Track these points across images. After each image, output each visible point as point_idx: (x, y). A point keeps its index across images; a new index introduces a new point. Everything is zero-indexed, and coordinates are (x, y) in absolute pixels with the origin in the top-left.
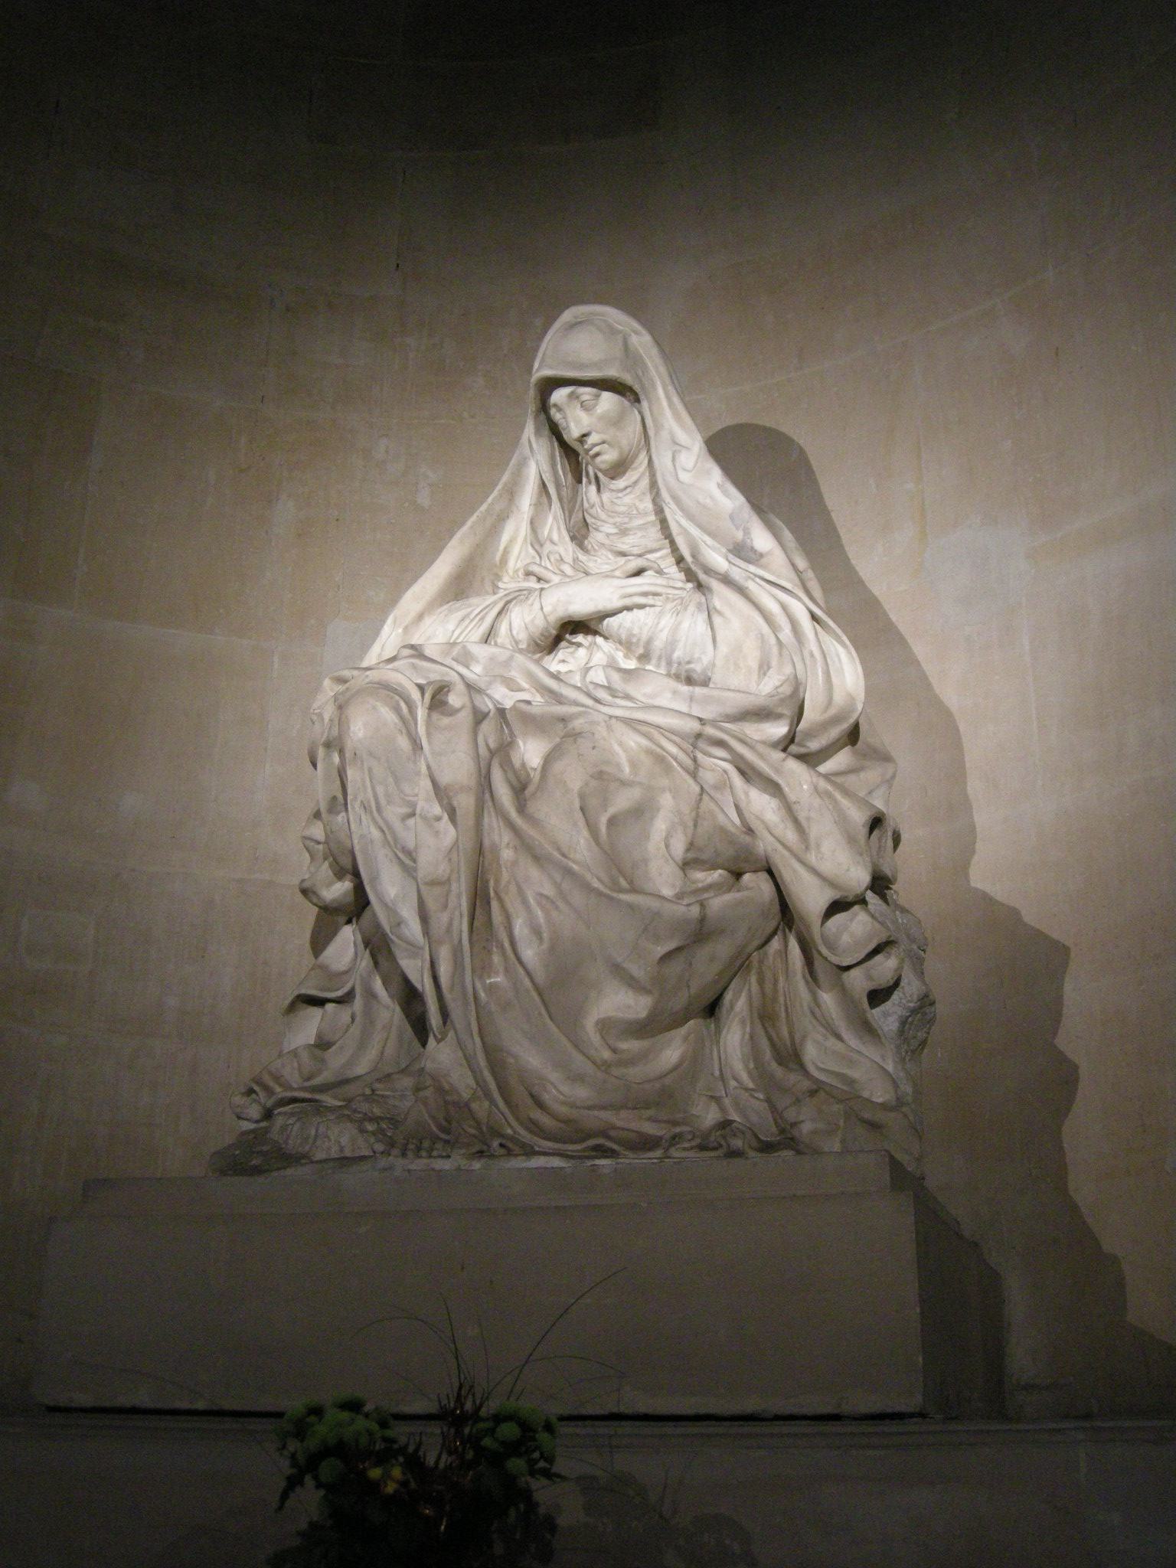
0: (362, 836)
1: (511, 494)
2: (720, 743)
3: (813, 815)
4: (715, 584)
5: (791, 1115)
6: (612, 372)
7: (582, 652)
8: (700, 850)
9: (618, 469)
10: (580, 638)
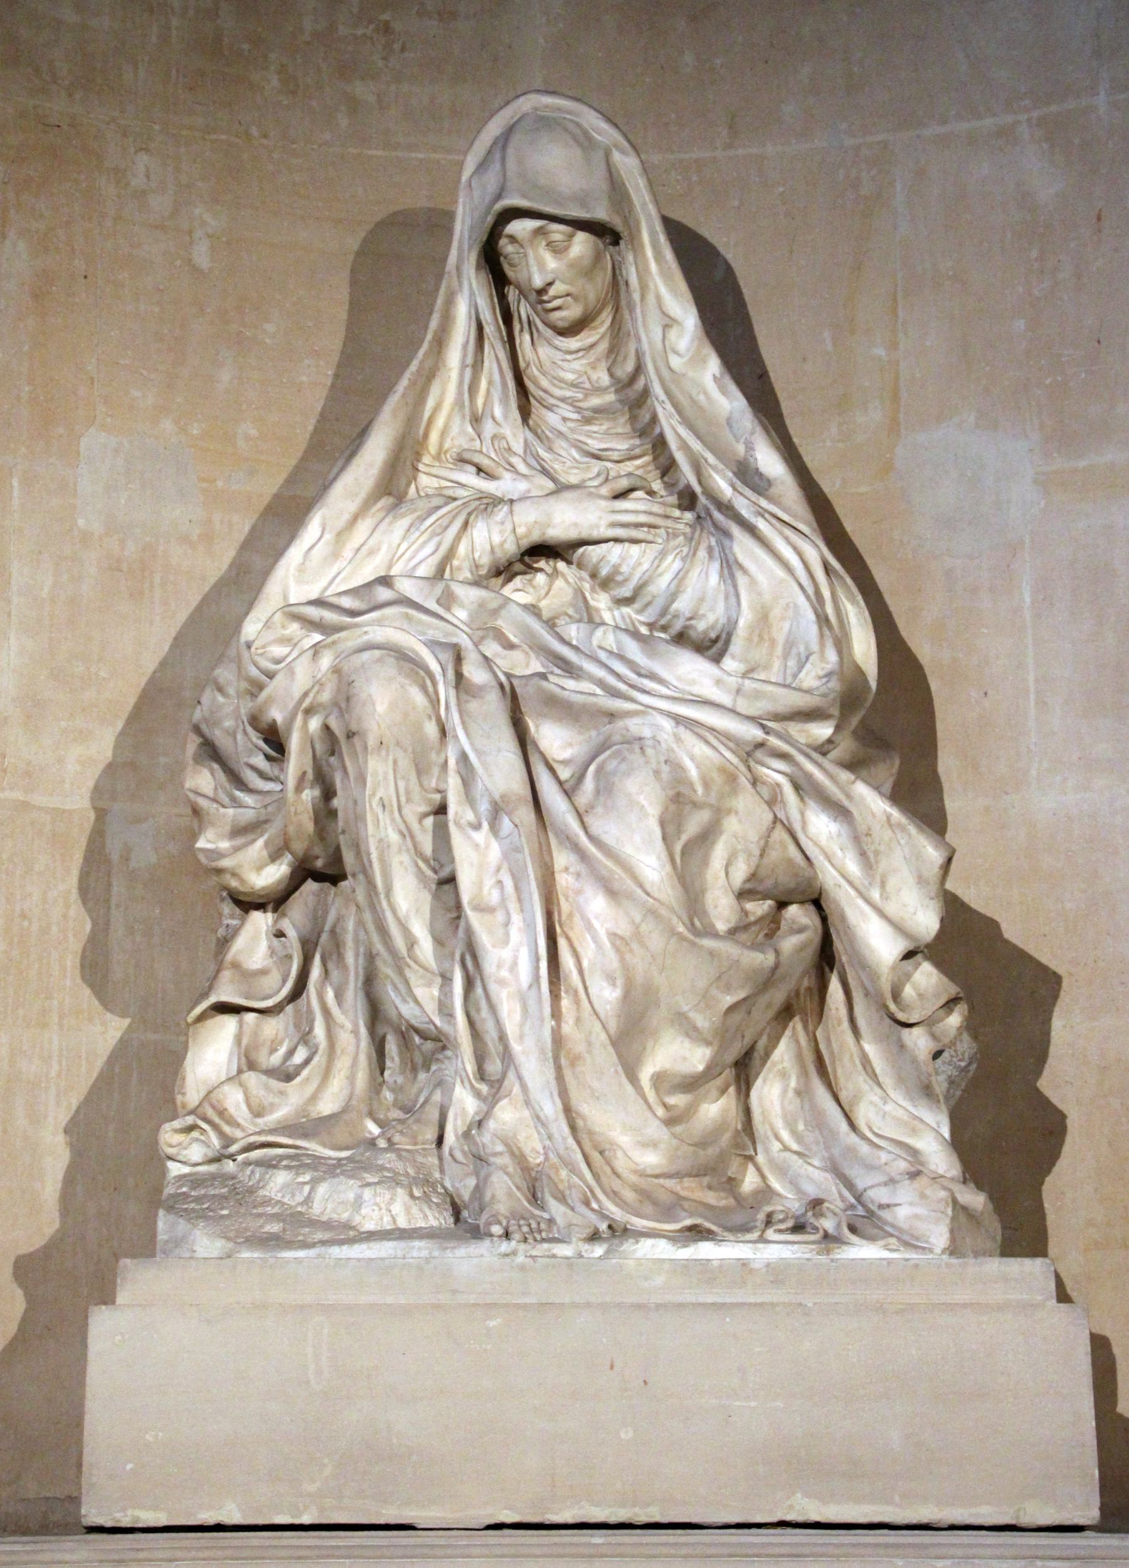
0: (381, 841)
1: (440, 343)
2: (783, 756)
3: (882, 848)
4: (736, 530)
5: (879, 1195)
6: (601, 213)
7: (540, 578)
8: (761, 881)
10: (542, 564)
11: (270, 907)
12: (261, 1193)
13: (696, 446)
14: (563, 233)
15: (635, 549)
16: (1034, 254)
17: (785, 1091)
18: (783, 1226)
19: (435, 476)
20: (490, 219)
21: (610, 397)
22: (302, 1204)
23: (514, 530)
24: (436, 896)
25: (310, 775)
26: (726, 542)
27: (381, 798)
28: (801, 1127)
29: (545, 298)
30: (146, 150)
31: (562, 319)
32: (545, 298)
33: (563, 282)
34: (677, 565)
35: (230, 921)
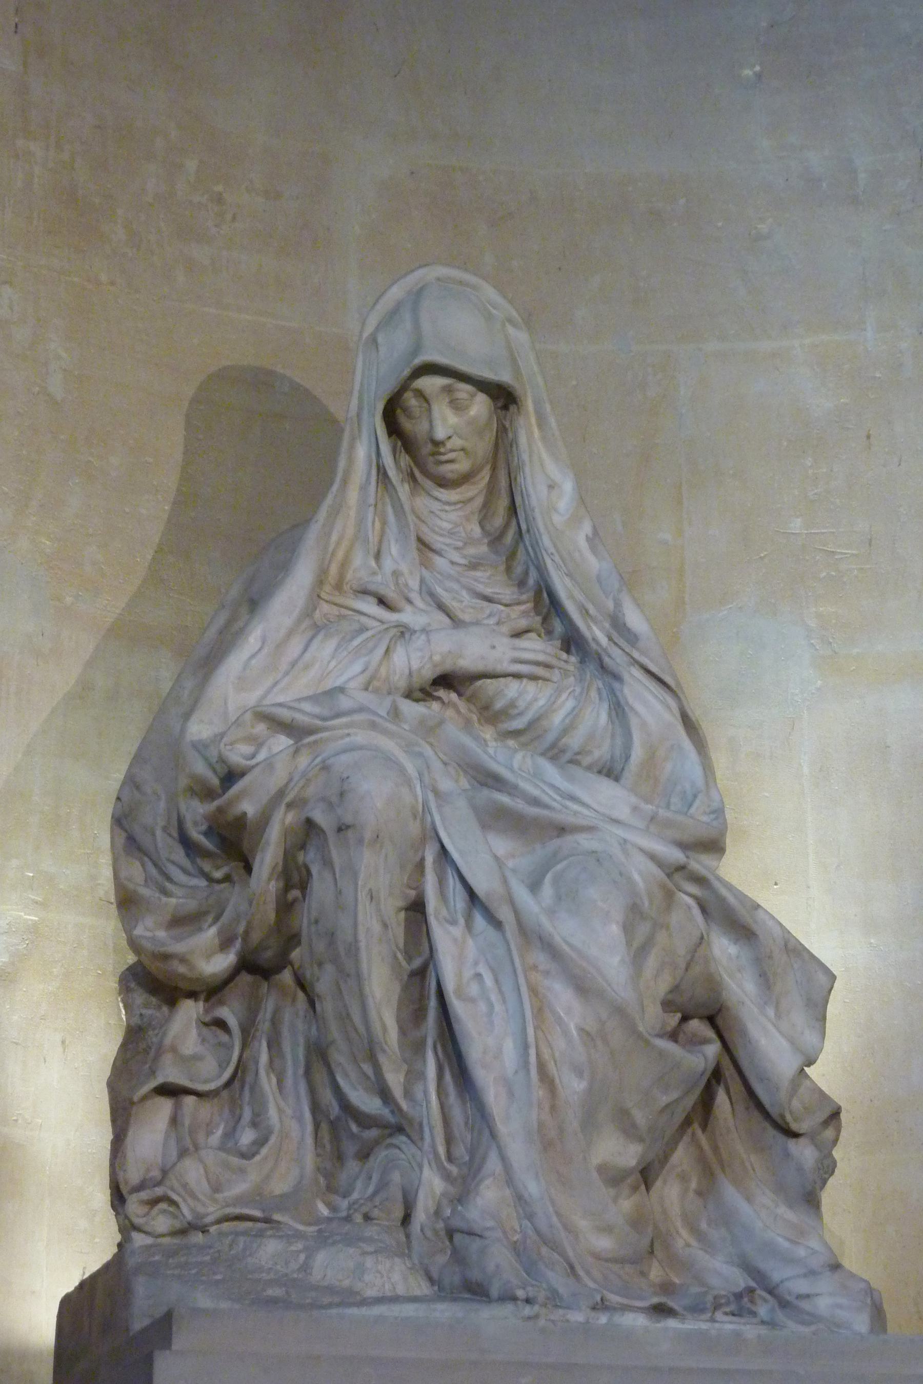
5: (801, 1286)
6: (504, 377)
11: (202, 997)
13: (580, 597)
14: (467, 392)
17: (685, 1191)
18: (728, 1310)
19: (335, 604)
20: (407, 372)
21: (484, 549)
22: (299, 1270)
23: (431, 657)
24: (405, 988)
25: (280, 868)
26: (616, 685)
27: (370, 890)
29: (442, 450)
30: (10, 283)
31: (452, 472)
33: (460, 437)
34: (570, 704)
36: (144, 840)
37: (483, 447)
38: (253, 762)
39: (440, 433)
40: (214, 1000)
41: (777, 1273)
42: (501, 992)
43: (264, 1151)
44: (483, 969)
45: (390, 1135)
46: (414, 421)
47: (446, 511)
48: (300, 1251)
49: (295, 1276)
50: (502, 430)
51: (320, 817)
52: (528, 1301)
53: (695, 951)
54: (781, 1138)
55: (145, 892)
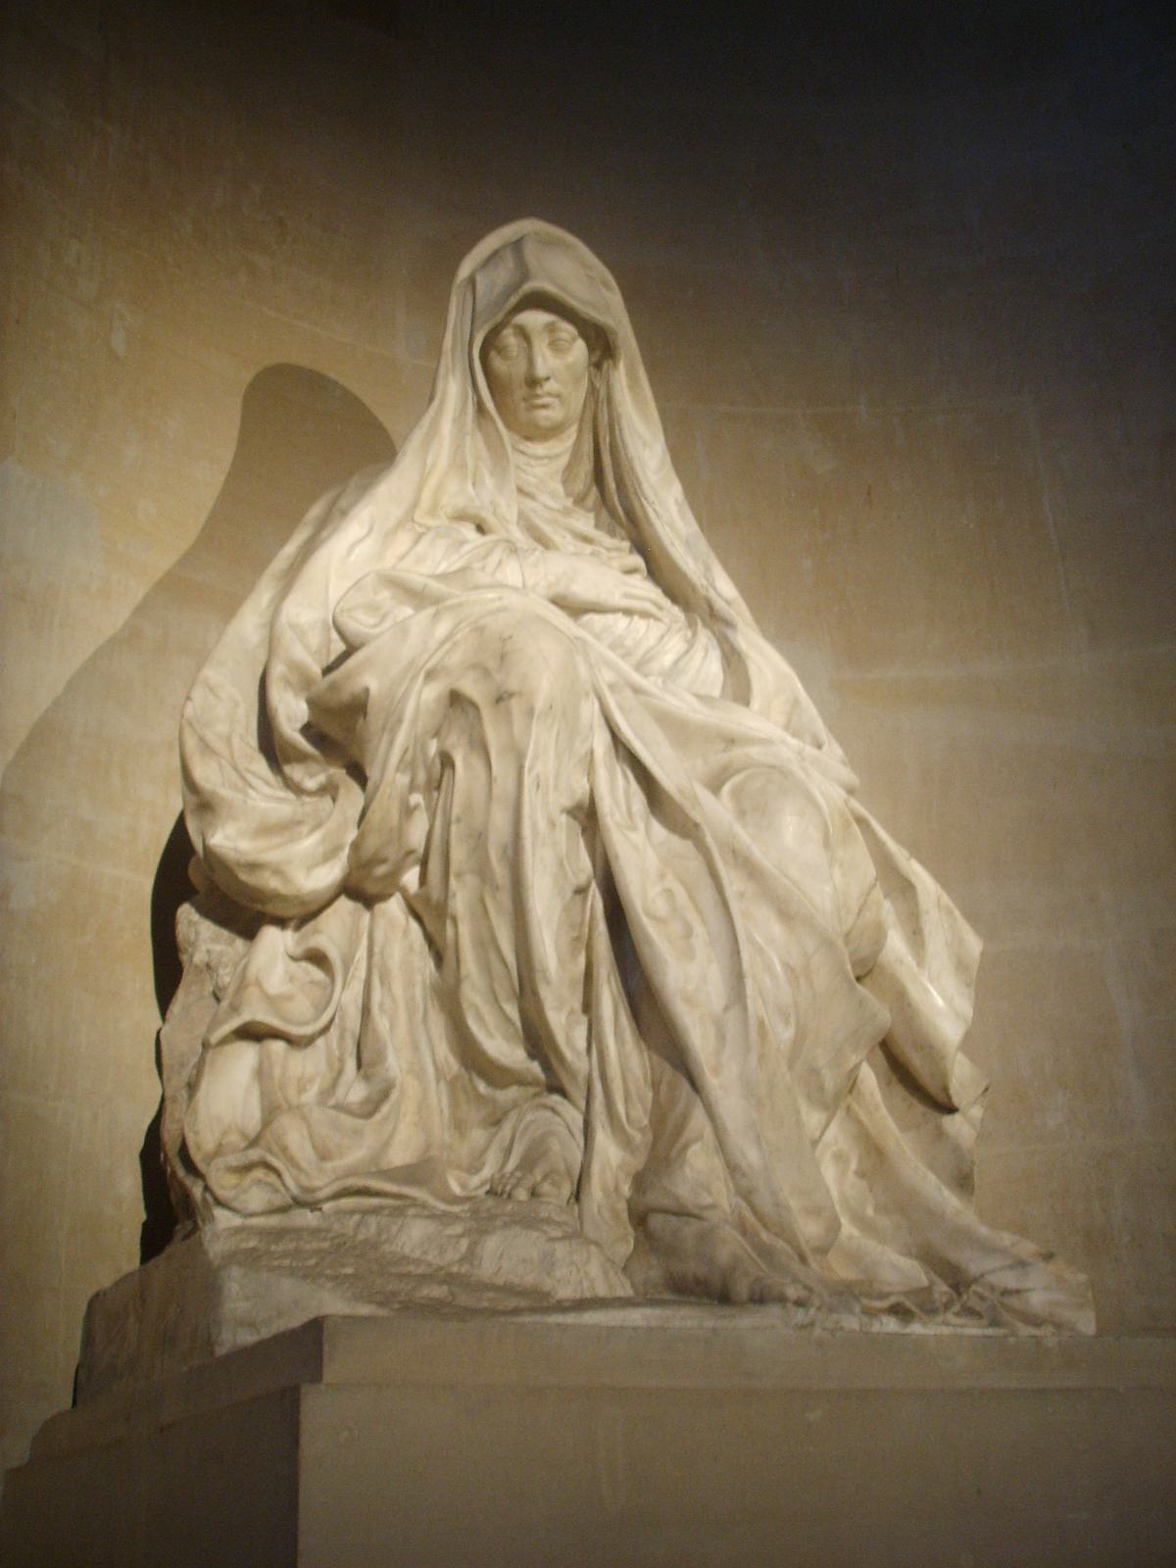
5: (1009, 1280)
9: (553, 432)
11: (292, 924)
12: (386, 1248)
15: (640, 624)
16: (816, 511)
22: (462, 1260)
24: (566, 909)
27: (538, 776)
28: (870, 1212)
31: (547, 418)
32: (539, 391)
33: (557, 381)
35: (212, 947)
36: (218, 745)
37: (578, 398)
38: (377, 630)
39: (541, 371)
40: (309, 927)
41: (974, 1263)
42: (699, 911)
43: (385, 1109)
44: (671, 882)
45: (536, 1095)
46: (509, 362)
47: (532, 466)
48: (461, 1236)
49: (455, 1269)
50: (593, 391)
51: (471, 688)
52: (800, 1303)
53: (868, 894)
54: (933, 1115)
55: (225, 792)
